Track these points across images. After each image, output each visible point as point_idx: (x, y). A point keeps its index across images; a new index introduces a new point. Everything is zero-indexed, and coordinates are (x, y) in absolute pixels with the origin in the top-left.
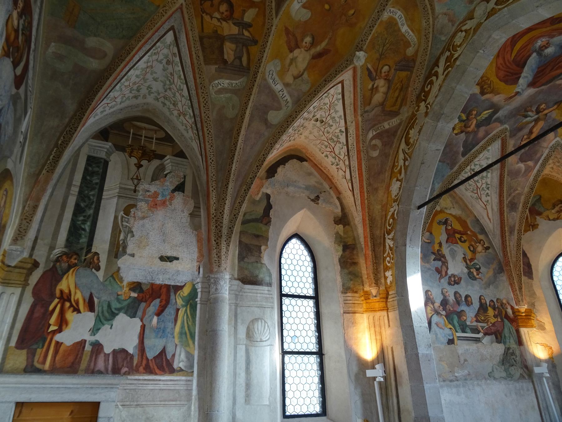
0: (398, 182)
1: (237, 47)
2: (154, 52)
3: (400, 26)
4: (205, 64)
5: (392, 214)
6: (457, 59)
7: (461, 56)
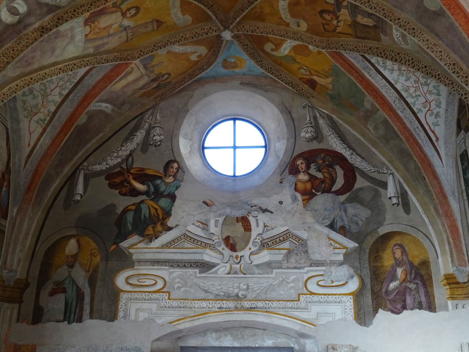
1: (359, 13)
2: (381, 64)
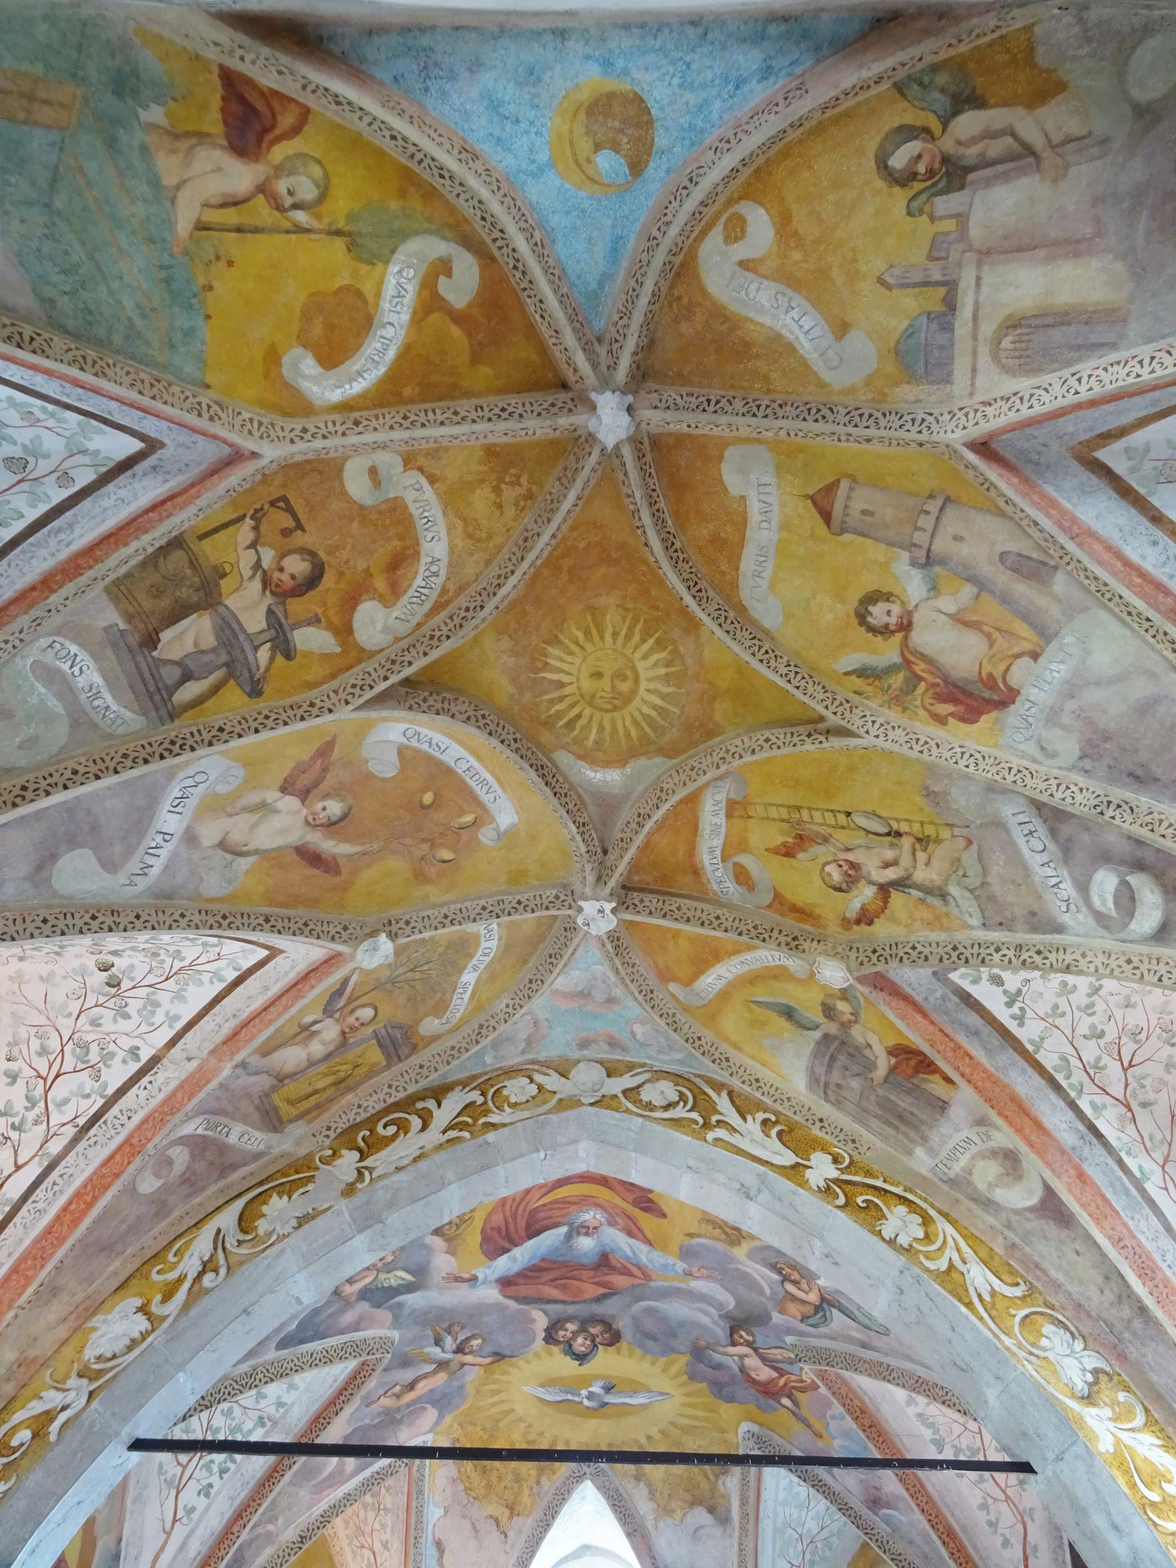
0: (140, 1317)
3: (469, 967)
4: (107, 589)
5: (47, 1412)
6: (493, 1126)
7: (506, 1130)
